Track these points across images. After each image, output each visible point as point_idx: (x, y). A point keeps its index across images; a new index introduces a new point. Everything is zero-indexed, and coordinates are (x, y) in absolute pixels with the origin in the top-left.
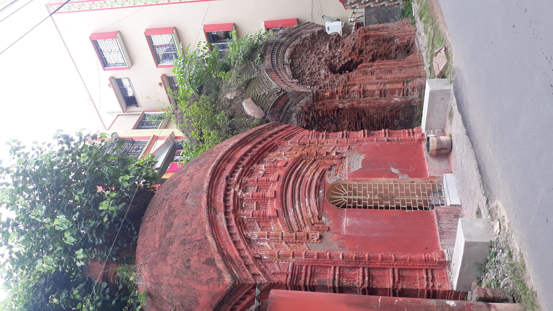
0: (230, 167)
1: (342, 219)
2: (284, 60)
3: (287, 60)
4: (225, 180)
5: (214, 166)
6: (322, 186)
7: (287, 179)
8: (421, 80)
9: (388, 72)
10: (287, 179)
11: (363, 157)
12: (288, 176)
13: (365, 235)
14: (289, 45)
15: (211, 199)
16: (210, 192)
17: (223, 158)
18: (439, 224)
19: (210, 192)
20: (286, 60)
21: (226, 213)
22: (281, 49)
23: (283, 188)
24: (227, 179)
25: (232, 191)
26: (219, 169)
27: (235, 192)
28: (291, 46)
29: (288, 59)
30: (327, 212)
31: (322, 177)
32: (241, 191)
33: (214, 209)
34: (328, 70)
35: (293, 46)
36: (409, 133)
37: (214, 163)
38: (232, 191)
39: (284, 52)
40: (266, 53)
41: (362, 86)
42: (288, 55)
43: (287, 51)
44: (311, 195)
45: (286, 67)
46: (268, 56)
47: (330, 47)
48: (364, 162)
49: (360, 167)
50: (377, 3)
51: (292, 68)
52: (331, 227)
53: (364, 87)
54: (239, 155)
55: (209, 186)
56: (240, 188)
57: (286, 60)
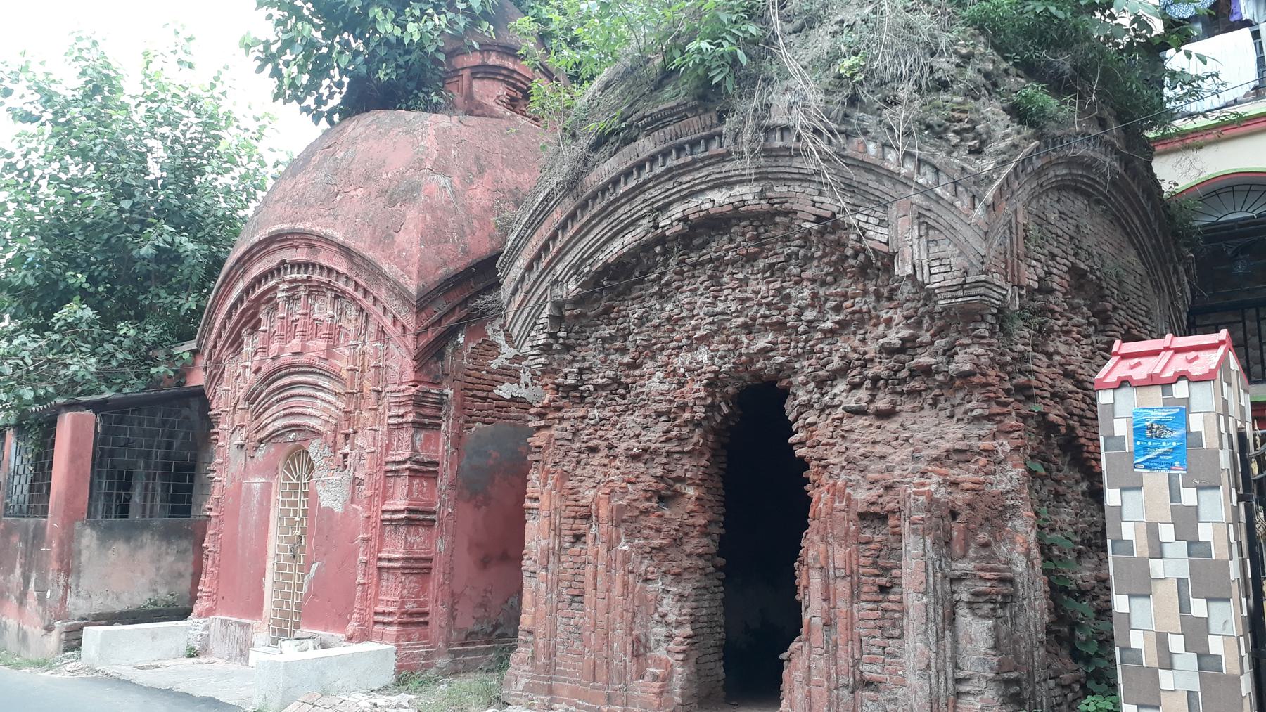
0: (301, 255)
1: (264, 476)
2: (675, 205)
3: (679, 215)
4: (278, 261)
5: (283, 229)
6: (302, 436)
7: (300, 369)
8: (521, 688)
9: (576, 592)
10: (300, 369)
11: (339, 510)
12: (307, 369)
13: (241, 512)
14: (776, 179)
15: (253, 256)
16: (255, 250)
17: (302, 234)
18: (236, 622)
19: (255, 250)
20: (677, 211)
21: (246, 291)
22: (729, 166)
23: (290, 367)
24: (284, 262)
25: (271, 283)
26: (287, 240)
27: (274, 288)
28: (780, 190)
29: (684, 219)
30: (272, 450)
31: (317, 434)
32: (284, 294)
33: (245, 272)
34: (708, 375)
35: (784, 199)
36: (390, 614)
37: (286, 226)
38: (271, 283)
39: (725, 183)
40: (656, 129)
41: (535, 505)
42: (708, 206)
43: (738, 190)
44: (287, 418)
45: (638, 231)
46: (646, 145)
47: (889, 351)
48: (330, 511)
49: (324, 504)
50: (1184, 606)
51: (658, 249)
52: (255, 460)
53: (534, 512)
54: (323, 259)
55: (260, 242)
56: (287, 291)
57: (677, 211)
